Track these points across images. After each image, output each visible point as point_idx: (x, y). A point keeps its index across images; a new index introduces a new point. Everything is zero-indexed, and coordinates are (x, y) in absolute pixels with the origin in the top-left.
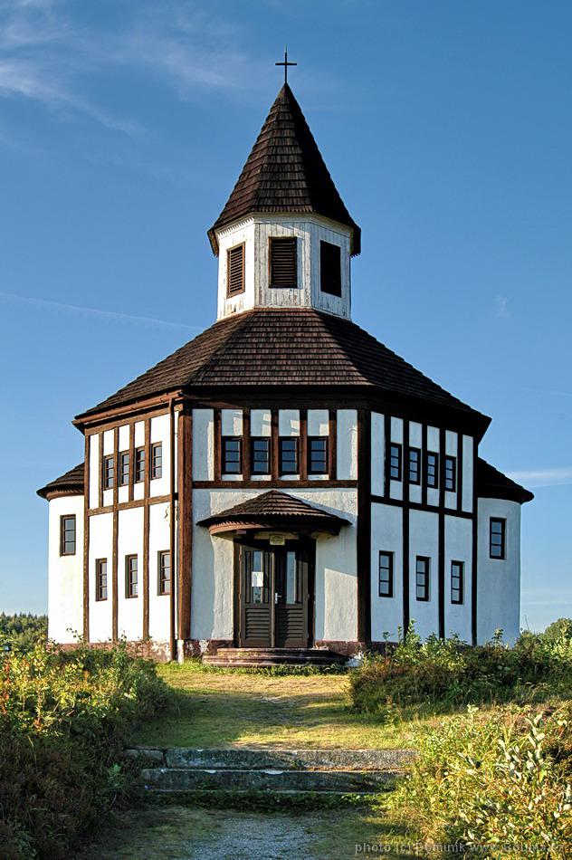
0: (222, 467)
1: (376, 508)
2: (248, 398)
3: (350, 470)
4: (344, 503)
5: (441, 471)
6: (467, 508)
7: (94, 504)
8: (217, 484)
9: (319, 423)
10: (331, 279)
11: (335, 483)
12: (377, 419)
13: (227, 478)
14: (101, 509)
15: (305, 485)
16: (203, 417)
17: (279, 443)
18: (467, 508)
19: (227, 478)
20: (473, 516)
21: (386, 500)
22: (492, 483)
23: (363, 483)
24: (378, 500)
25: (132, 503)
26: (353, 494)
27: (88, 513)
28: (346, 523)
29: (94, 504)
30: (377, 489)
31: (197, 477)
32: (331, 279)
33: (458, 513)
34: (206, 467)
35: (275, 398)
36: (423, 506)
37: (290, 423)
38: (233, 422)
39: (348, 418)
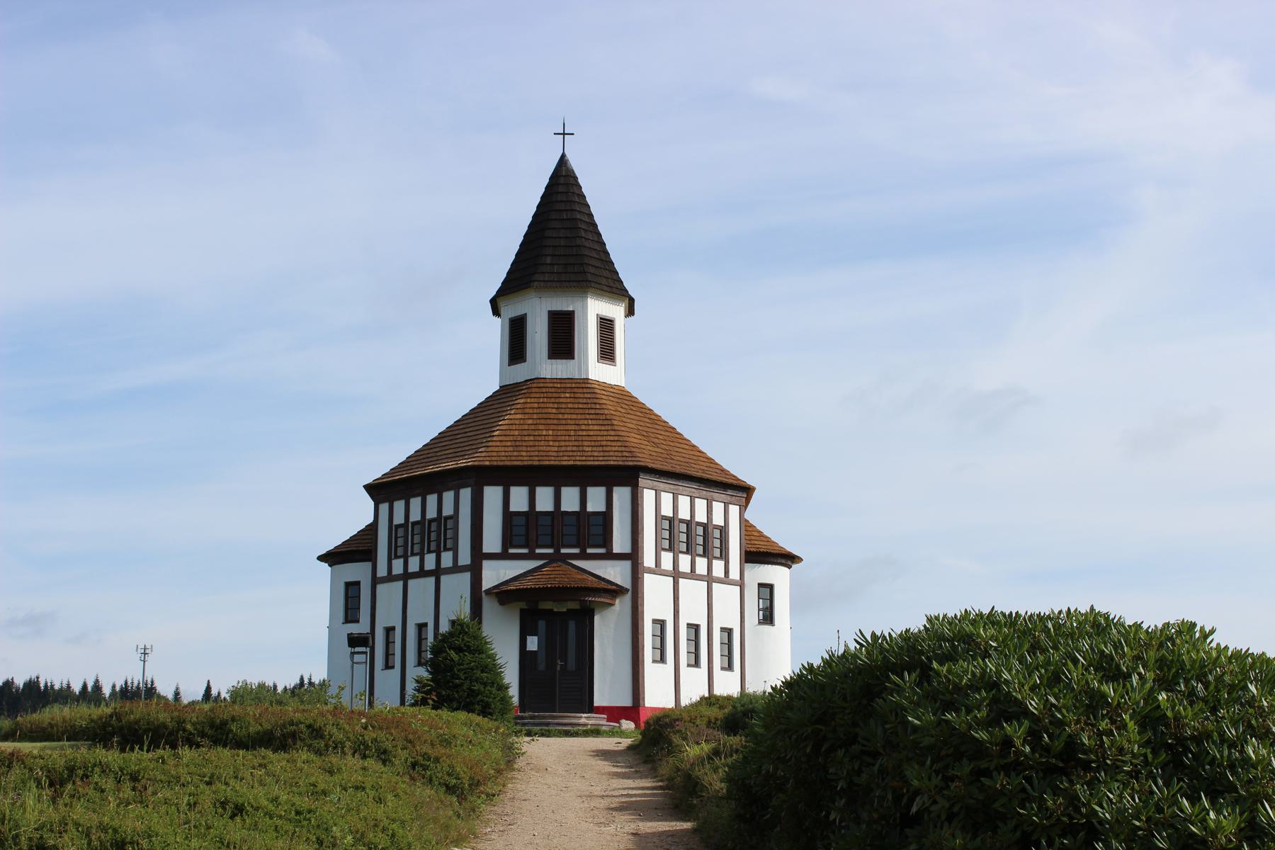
0: (508, 541)
1: (648, 579)
2: (532, 476)
4: (616, 573)
5: (706, 541)
6: (734, 574)
7: (382, 571)
8: (503, 556)
9: (596, 499)
10: (607, 353)
11: (610, 556)
12: (648, 497)
13: (511, 551)
14: (390, 578)
15: (584, 556)
16: (492, 495)
17: (558, 514)
18: (734, 574)
19: (511, 551)
20: (741, 584)
21: (657, 570)
22: (761, 553)
23: (634, 556)
24: (651, 571)
25: (422, 573)
26: (627, 565)
27: (375, 581)
28: (627, 590)
29: (382, 571)
30: (648, 560)
32: (607, 353)
33: (726, 580)
35: (558, 476)
36: (692, 575)
37: (570, 499)
38: (519, 499)
39: (621, 495)
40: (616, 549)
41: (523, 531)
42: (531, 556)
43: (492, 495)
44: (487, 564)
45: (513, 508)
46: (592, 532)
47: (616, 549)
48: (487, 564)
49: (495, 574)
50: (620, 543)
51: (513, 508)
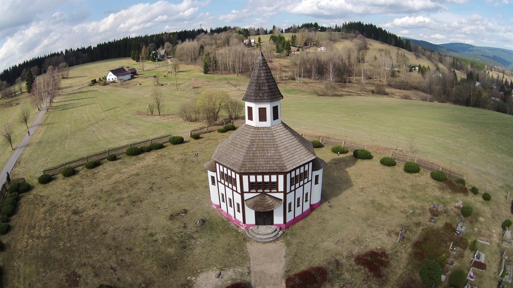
3: (281, 188)
8: (249, 192)
9: (274, 178)
11: (278, 192)
16: (245, 178)
31: (244, 191)
34: (246, 188)
38: (253, 179)
40: (279, 191)
41: (253, 186)
42: (257, 192)
43: (245, 178)
44: (245, 194)
45: (251, 181)
46: (274, 186)
47: (279, 191)
48: (245, 194)
49: (247, 196)
50: (281, 188)
51: (251, 181)
